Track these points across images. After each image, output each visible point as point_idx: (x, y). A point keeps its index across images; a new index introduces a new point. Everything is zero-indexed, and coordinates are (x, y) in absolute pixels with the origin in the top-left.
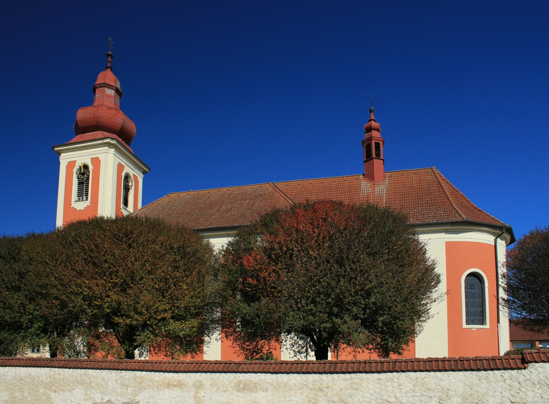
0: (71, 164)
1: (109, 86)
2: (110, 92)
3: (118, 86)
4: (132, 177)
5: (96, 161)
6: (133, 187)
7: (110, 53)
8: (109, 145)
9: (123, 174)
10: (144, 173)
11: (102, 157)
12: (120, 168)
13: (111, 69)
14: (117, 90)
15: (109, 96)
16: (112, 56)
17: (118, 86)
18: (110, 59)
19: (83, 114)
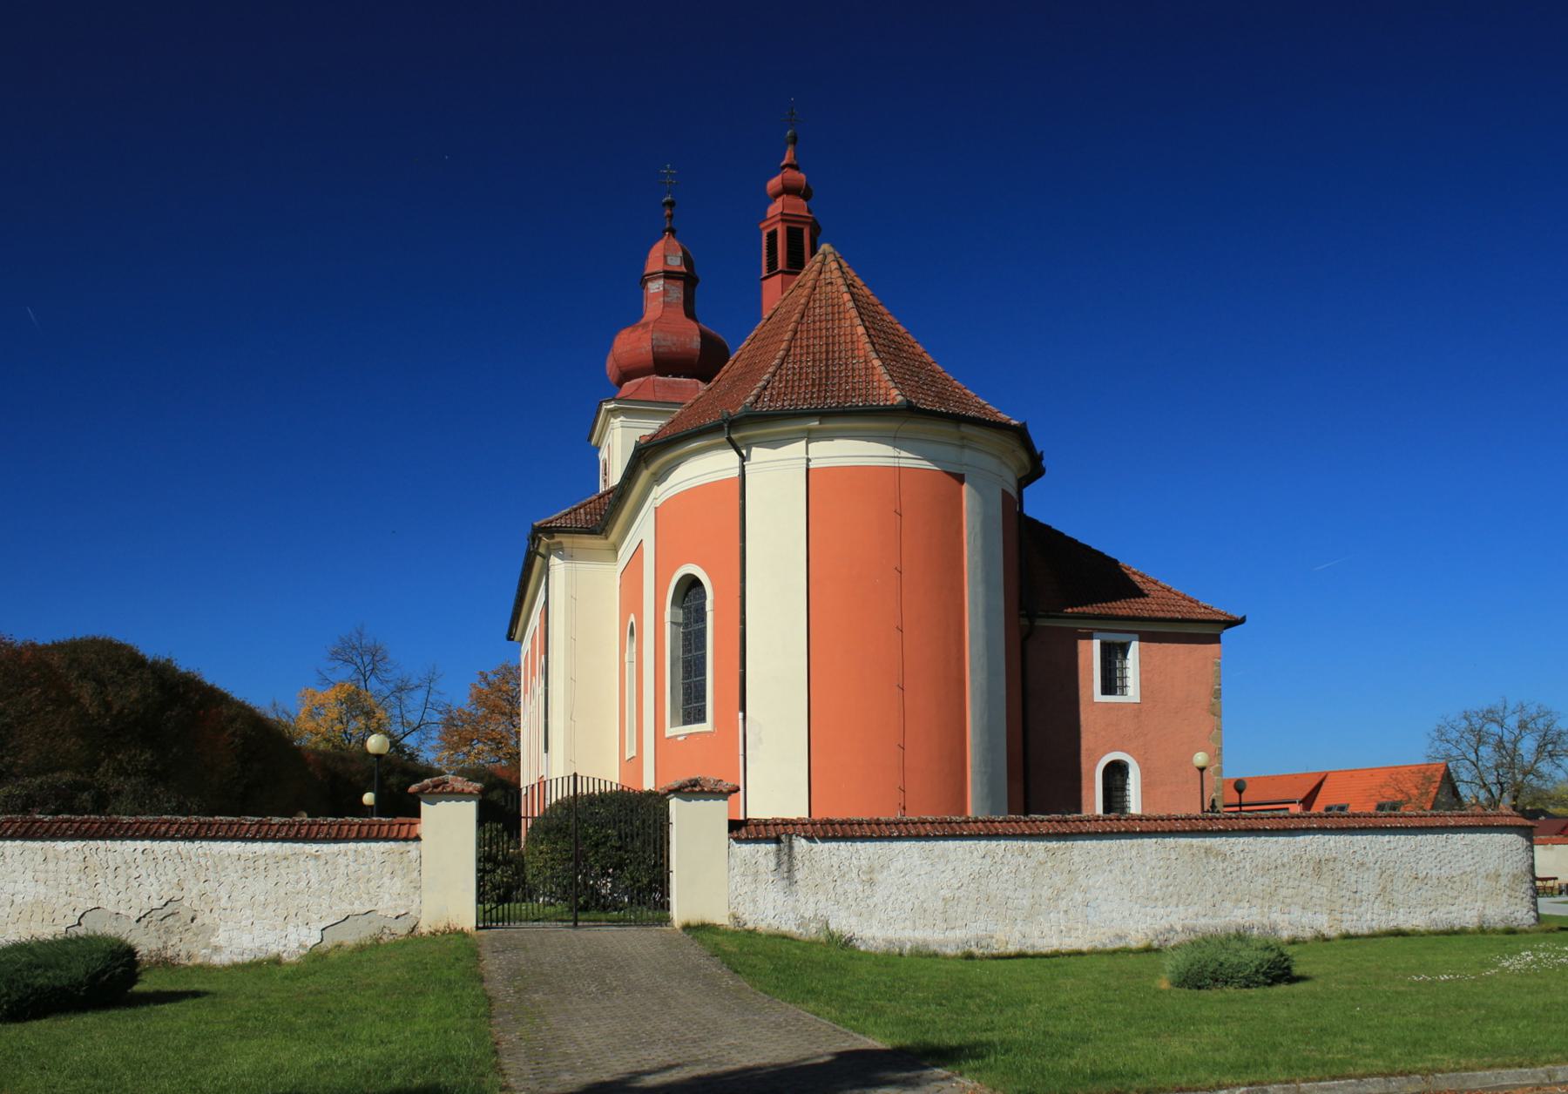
1: (654, 276)
3: (676, 262)
7: (669, 198)
8: (613, 413)
13: (672, 231)
14: (669, 275)
16: (671, 204)
17: (676, 262)
18: (668, 212)
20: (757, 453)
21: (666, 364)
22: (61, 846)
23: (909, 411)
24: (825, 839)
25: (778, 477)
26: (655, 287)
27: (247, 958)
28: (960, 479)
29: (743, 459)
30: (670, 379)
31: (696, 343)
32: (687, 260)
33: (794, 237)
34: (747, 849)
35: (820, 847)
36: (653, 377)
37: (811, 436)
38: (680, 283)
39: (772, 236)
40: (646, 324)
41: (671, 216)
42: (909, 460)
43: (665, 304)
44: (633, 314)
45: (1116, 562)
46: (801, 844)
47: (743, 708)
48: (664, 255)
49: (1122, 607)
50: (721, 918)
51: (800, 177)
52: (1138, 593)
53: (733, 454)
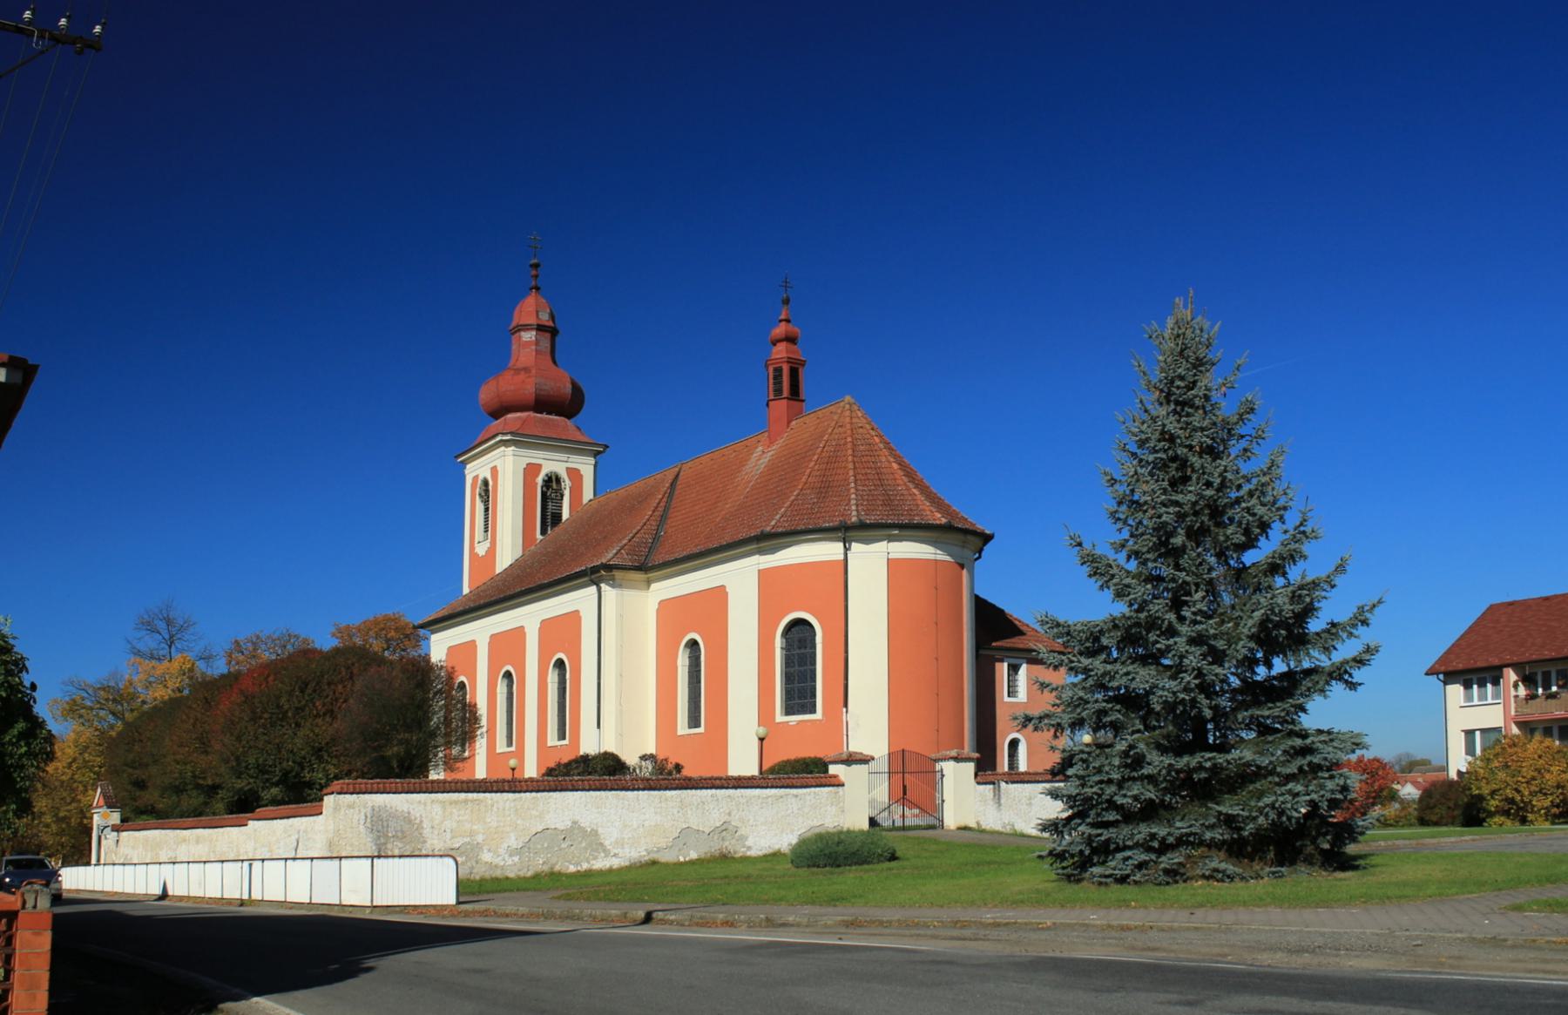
0: (476, 478)
1: (526, 327)
2: (528, 336)
3: (545, 317)
4: (564, 475)
5: (494, 470)
6: (567, 493)
7: (534, 261)
9: (540, 480)
10: (596, 454)
11: (498, 463)
12: (531, 470)
13: (537, 289)
14: (540, 328)
15: (528, 344)
16: (536, 266)
17: (545, 317)
19: (487, 393)
20: (855, 546)
21: (543, 404)
22: (669, 793)
23: (949, 528)
24: (1013, 782)
25: (870, 566)
26: (528, 336)
27: (765, 852)
28: (962, 566)
29: (846, 549)
30: (544, 416)
31: (568, 389)
32: (552, 317)
33: (794, 374)
34: (982, 787)
35: (1011, 786)
36: (531, 414)
37: (891, 539)
38: (548, 335)
39: (778, 371)
40: (526, 370)
41: (536, 276)
42: (941, 556)
43: (537, 352)
44: (500, 359)
45: (1002, 611)
46: (1003, 785)
47: (846, 705)
48: (531, 309)
49: (1016, 642)
50: (973, 825)
51: (793, 328)
52: (1021, 633)
53: (841, 545)
